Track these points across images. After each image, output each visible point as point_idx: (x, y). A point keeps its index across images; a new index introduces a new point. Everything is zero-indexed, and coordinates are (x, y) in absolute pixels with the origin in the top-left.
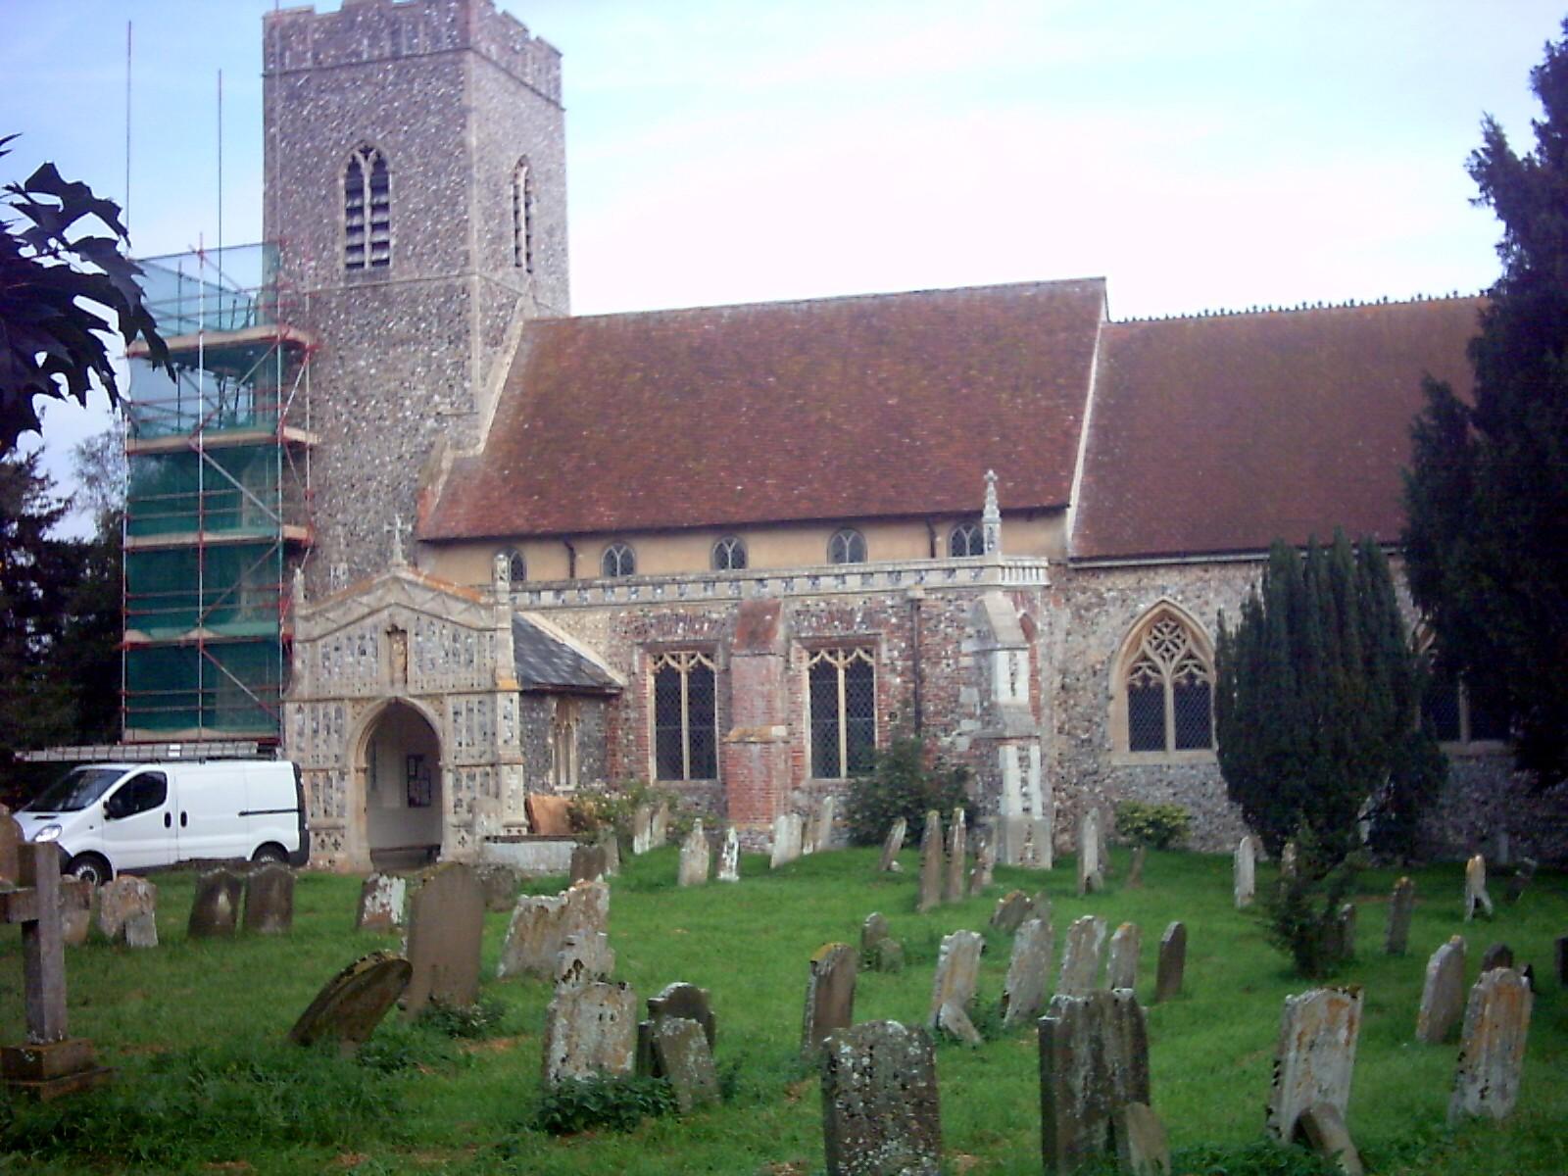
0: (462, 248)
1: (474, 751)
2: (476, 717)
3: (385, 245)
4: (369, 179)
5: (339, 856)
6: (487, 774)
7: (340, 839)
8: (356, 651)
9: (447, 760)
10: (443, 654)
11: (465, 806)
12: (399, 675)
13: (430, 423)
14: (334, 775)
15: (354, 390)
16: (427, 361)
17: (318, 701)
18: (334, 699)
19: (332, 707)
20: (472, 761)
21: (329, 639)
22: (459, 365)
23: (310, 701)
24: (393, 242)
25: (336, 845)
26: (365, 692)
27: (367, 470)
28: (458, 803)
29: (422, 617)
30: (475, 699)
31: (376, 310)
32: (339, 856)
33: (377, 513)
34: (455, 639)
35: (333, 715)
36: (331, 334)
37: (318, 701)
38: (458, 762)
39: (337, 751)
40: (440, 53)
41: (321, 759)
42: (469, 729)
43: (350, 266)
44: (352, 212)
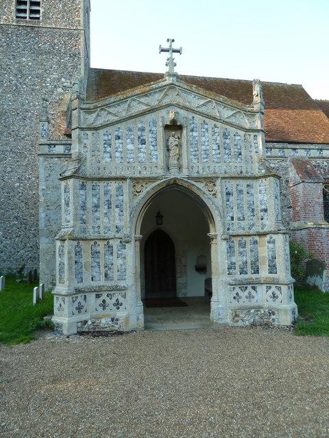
0: (78, 19)
1: (243, 223)
2: (245, 196)
3: (38, 12)
5: (121, 314)
6: (256, 242)
8: (136, 141)
9: (217, 230)
10: (215, 147)
11: (237, 268)
12: (173, 161)
13: (60, 90)
14: (115, 244)
15: (20, 71)
16: (59, 63)
17: (100, 179)
18: (116, 179)
19: (113, 186)
20: (242, 232)
22: (75, 67)
23: (92, 179)
26: (145, 174)
28: (232, 266)
29: (196, 116)
30: (243, 184)
31: (33, 37)
32: (121, 314)
33: (31, 127)
34: (225, 136)
35: (113, 192)
37: (100, 179)
38: (231, 232)
39: (117, 222)
41: (102, 230)
42: (240, 207)
43: (17, 17)
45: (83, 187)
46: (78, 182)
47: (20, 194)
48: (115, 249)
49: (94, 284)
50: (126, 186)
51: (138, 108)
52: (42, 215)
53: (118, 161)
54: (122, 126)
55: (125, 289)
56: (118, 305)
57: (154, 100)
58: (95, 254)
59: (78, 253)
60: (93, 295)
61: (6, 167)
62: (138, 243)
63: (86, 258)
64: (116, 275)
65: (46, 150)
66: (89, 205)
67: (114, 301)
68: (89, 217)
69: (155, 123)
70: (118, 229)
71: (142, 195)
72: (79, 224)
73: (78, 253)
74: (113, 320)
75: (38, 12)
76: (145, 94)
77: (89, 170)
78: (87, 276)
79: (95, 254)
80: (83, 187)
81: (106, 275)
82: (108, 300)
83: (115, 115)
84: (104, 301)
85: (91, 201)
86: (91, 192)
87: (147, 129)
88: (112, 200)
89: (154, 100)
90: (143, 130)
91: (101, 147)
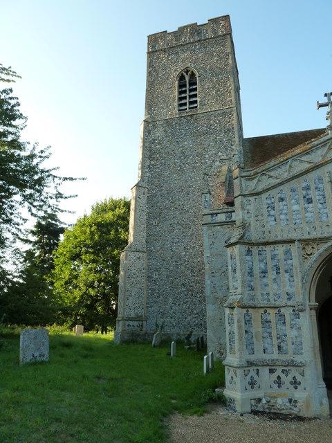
3: (196, 102)
4: (187, 83)
5: (299, 395)
7: (299, 378)
8: (302, 201)
13: (217, 163)
14: (287, 312)
16: (215, 141)
19: (280, 250)
21: (272, 192)
22: (230, 140)
23: (258, 244)
24: (198, 99)
25: (295, 383)
26: (315, 235)
27: (189, 183)
32: (299, 395)
36: (173, 133)
39: (288, 289)
40: (217, 37)
41: (271, 297)
43: (179, 110)
44: (180, 93)
45: (249, 252)
46: (244, 248)
47: (186, 263)
48: (288, 318)
49: (267, 357)
50: (295, 249)
51: (299, 167)
52: (208, 282)
53: (284, 223)
54: (286, 187)
55: (303, 365)
56: (295, 383)
57: (317, 157)
58: (266, 323)
59: (248, 322)
60: (267, 369)
61: (174, 238)
62: (314, 312)
63: (257, 327)
64: (290, 348)
65: (209, 219)
66: (257, 271)
67: (290, 378)
68: (257, 282)
69: (320, 180)
70: (289, 297)
71: (314, 258)
72: (247, 292)
73: (248, 322)
74: (290, 401)
75: (196, 102)
76: (307, 152)
77: (254, 235)
78: (258, 347)
79: (266, 323)
80: (249, 252)
81: (279, 348)
82: (283, 376)
83: (276, 178)
84: (279, 378)
85: (258, 266)
86: (257, 258)
87: (313, 187)
88: (281, 265)
89: (317, 157)
90: (308, 188)
91: (265, 212)
